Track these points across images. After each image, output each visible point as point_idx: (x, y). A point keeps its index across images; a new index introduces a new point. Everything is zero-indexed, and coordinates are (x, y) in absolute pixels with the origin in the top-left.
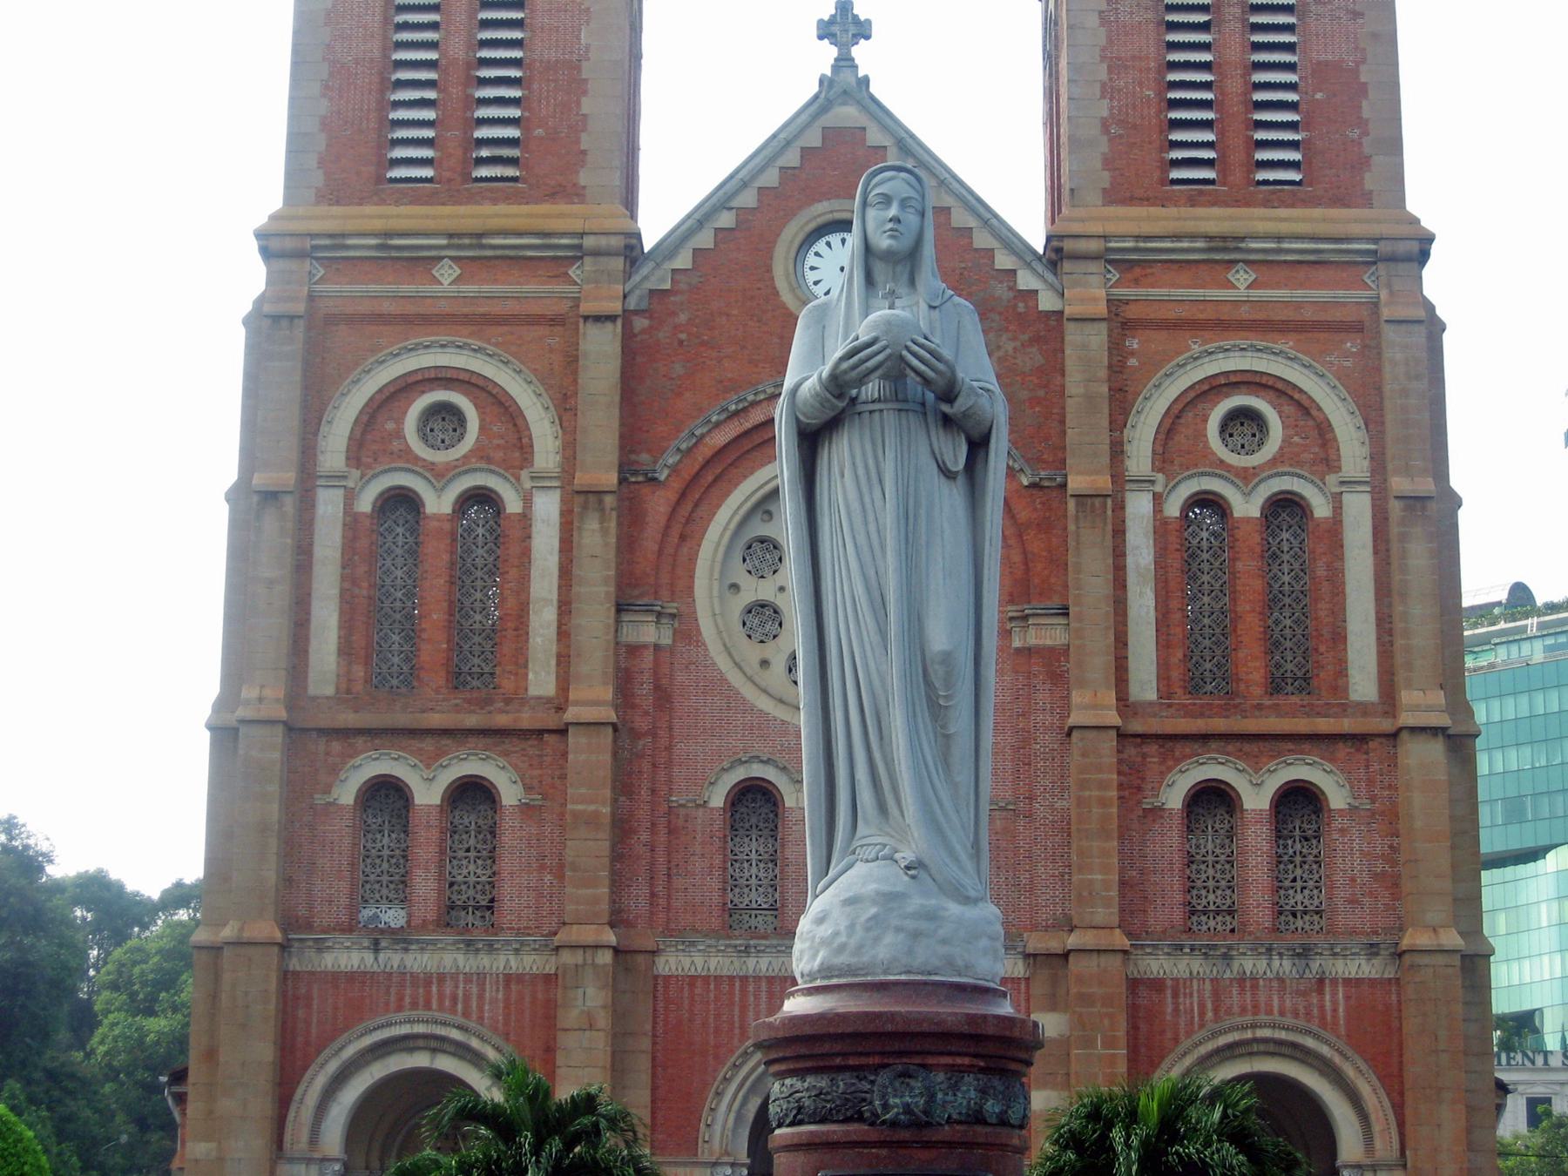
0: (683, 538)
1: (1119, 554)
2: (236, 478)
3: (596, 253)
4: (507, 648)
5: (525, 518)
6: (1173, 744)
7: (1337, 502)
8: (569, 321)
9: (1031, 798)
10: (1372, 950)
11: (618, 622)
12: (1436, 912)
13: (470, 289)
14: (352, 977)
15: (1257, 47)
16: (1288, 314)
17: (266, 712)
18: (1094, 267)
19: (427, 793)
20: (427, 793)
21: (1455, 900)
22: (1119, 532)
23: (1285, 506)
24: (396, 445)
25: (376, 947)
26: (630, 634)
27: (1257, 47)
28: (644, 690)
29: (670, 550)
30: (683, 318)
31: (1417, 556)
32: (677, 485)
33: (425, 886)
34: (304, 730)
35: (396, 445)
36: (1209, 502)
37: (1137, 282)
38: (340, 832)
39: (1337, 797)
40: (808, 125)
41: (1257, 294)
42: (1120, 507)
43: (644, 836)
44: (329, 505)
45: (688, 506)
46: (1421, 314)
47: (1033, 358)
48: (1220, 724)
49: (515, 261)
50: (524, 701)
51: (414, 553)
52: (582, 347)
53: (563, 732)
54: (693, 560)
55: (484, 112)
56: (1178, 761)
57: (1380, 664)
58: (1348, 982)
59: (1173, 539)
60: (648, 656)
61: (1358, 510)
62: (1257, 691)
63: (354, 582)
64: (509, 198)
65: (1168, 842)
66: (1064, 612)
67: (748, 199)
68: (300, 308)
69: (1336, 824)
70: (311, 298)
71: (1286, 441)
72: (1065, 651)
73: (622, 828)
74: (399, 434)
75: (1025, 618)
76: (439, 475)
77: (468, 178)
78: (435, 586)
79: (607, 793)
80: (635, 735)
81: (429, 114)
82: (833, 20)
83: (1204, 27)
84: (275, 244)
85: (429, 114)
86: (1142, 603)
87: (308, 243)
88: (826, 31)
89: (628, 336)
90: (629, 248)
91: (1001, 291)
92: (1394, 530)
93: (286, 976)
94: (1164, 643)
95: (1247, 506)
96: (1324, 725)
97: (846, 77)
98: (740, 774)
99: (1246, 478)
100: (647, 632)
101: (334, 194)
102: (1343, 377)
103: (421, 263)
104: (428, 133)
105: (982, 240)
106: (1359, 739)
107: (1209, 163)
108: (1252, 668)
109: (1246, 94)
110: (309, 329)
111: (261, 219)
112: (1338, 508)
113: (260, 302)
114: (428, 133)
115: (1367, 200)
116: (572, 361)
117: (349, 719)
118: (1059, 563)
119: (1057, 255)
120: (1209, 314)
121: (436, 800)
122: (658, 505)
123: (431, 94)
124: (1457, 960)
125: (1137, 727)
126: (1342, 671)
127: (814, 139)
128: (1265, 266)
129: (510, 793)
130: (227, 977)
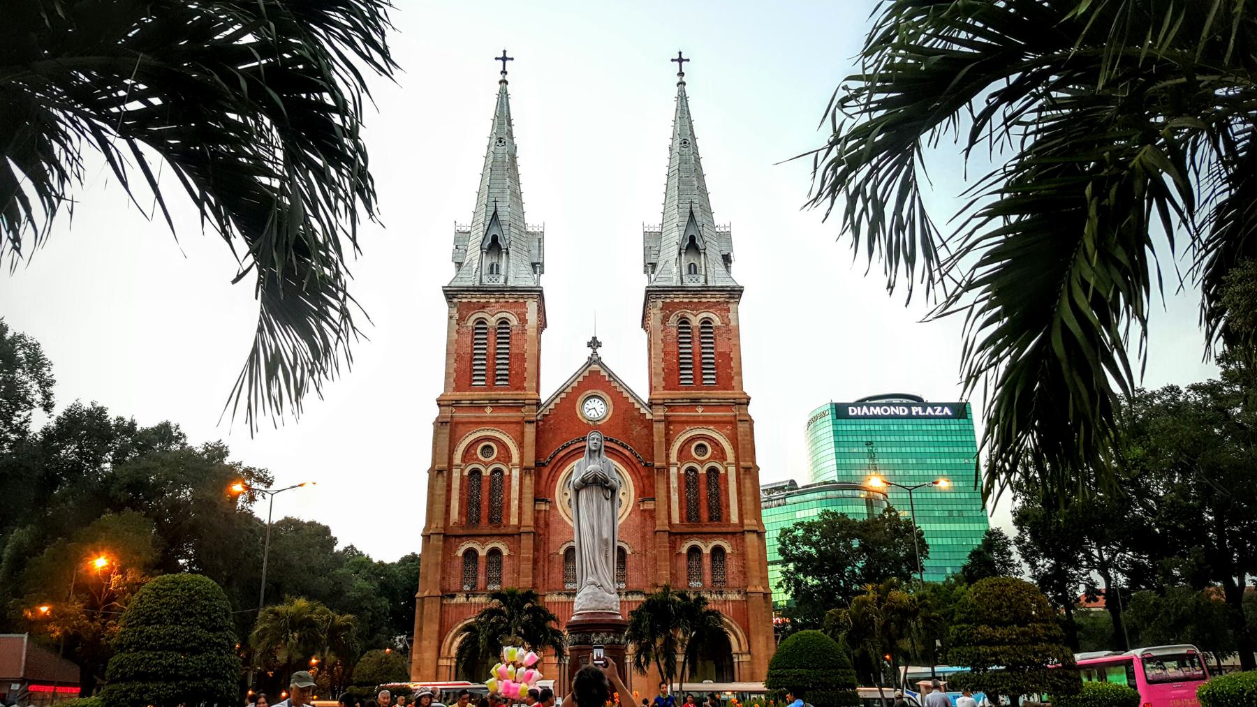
0: (552, 480)
1: (668, 484)
2: (429, 466)
3: (529, 405)
4: (504, 512)
5: (510, 476)
6: (684, 536)
7: (726, 469)
8: (522, 423)
9: (646, 551)
10: (739, 592)
11: (535, 504)
12: (756, 582)
13: (495, 414)
14: (461, 605)
15: (703, 348)
16: (712, 419)
17: (438, 531)
18: (661, 407)
19: (482, 553)
20: (482, 553)
21: (762, 578)
22: (668, 478)
23: (713, 471)
24: (475, 457)
25: (468, 597)
26: (537, 508)
27: (703, 348)
28: (542, 522)
29: (549, 484)
30: (552, 421)
31: (748, 483)
32: (550, 466)
33: (481, 578)
34: (449, 536)
35: (475, 457)
36: (692, 469)
37: (672, 411)
38: (458, 564)
39: (728, 550)
40: (585, 370)
41: (704, 414)
42: (668, 471)
43: (541, 562)
44: (456, 474)
45: (553, 474)
46: (748, 418)
47: (645, 431)
48: (696, 530)
49: (507, 407)
50: (509, 526)
51: (479, 486)
52: (526, 430)
53: (520, 534)
54: (555, 487)
55: (498, 367)
56: (685, 539)
57: (739, 513)
58: (732, 601)
59: (683, 481)
60: (543, 513)
61: (732, 470)
62: (706, 520)
63: (463, 494)
64: (505, 390)
65: (683, 563)
66: (654, 500)
67: (569, 390)
68: (449, 420)
69: (729, 557)
70: (452, 417)
71: (712, 453)
72: (655, 510)
73: (535, 561)
74: (476, 454)
75: (643, 501)
76: (486, 465)
77: (494, 384)
78: (485, 495)
79: (532, 551)
80: (541, 535)
81: (484, 367)
82: (591, 343)
83: (689, 343)
84: (442, 403)
85: (484, 367)
86: (675, 497)
87: (451, 403)
88: (589, 345)
89: (537, 426)
90: (538, 403)
91: (636, 413)
92: (742, 477)
93: (442, 605)
94: (681, 508)
95: (702, 471)
96: (724, 530)
97: (595, 358)
98: (567, 545)
99: (702, 463)
100: (543, 507)
101: (457, 389)
102: (727, 436)
103: (482, 408)
104: (484, 373)
105: (631, 400)
106: (734, 534)
107: (691, 379)
108: (705, 515)
109: (700, 361)
110: (451, 425)
111: (438, 396)
112: (726, 471)
113: (437, 419)
114: (484, 373)
115: (733, 388)
116: (523, 433)
117: (461, 532)
118: (653, 487)
119: (651, 405)
120: (691, 419)
121: (485, 554)
122: (546, 472)
123: (485, 362)
124: (762, 595)
125: (674, 531)
126: (729, 515)
127: (586, 373)
128: (707, 407)
129: (505, 552)
130: (426, 607)
